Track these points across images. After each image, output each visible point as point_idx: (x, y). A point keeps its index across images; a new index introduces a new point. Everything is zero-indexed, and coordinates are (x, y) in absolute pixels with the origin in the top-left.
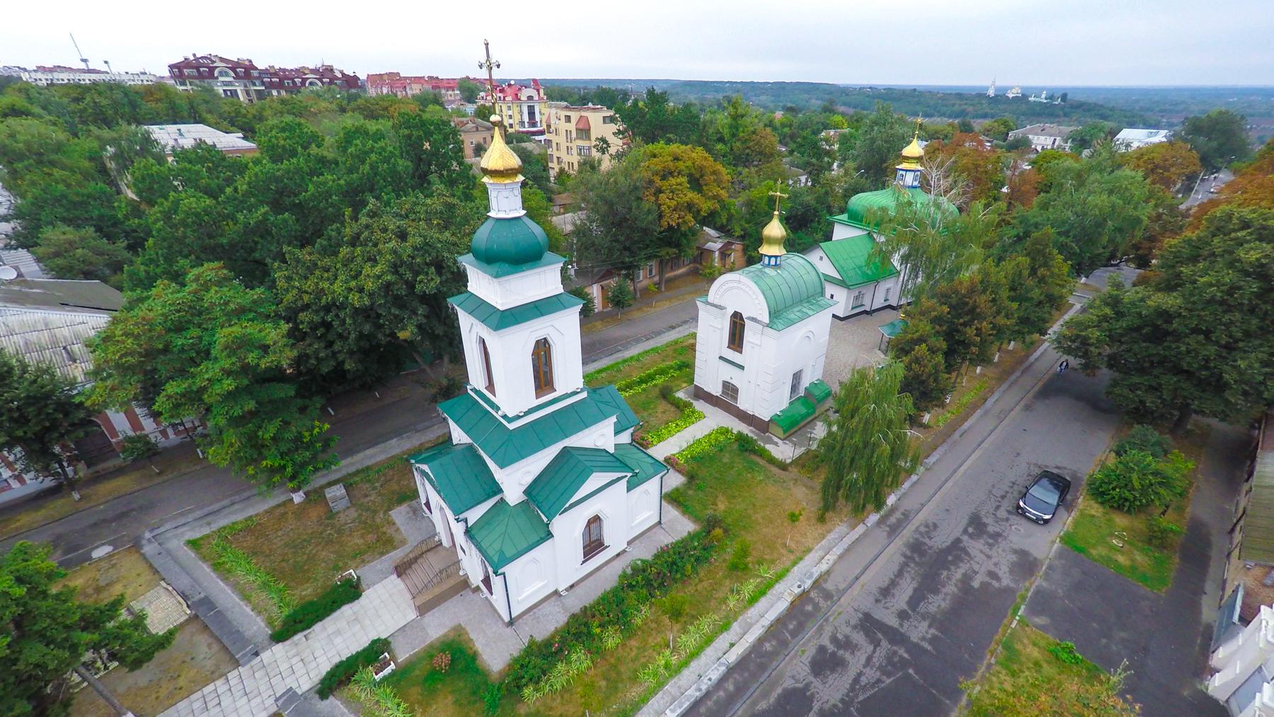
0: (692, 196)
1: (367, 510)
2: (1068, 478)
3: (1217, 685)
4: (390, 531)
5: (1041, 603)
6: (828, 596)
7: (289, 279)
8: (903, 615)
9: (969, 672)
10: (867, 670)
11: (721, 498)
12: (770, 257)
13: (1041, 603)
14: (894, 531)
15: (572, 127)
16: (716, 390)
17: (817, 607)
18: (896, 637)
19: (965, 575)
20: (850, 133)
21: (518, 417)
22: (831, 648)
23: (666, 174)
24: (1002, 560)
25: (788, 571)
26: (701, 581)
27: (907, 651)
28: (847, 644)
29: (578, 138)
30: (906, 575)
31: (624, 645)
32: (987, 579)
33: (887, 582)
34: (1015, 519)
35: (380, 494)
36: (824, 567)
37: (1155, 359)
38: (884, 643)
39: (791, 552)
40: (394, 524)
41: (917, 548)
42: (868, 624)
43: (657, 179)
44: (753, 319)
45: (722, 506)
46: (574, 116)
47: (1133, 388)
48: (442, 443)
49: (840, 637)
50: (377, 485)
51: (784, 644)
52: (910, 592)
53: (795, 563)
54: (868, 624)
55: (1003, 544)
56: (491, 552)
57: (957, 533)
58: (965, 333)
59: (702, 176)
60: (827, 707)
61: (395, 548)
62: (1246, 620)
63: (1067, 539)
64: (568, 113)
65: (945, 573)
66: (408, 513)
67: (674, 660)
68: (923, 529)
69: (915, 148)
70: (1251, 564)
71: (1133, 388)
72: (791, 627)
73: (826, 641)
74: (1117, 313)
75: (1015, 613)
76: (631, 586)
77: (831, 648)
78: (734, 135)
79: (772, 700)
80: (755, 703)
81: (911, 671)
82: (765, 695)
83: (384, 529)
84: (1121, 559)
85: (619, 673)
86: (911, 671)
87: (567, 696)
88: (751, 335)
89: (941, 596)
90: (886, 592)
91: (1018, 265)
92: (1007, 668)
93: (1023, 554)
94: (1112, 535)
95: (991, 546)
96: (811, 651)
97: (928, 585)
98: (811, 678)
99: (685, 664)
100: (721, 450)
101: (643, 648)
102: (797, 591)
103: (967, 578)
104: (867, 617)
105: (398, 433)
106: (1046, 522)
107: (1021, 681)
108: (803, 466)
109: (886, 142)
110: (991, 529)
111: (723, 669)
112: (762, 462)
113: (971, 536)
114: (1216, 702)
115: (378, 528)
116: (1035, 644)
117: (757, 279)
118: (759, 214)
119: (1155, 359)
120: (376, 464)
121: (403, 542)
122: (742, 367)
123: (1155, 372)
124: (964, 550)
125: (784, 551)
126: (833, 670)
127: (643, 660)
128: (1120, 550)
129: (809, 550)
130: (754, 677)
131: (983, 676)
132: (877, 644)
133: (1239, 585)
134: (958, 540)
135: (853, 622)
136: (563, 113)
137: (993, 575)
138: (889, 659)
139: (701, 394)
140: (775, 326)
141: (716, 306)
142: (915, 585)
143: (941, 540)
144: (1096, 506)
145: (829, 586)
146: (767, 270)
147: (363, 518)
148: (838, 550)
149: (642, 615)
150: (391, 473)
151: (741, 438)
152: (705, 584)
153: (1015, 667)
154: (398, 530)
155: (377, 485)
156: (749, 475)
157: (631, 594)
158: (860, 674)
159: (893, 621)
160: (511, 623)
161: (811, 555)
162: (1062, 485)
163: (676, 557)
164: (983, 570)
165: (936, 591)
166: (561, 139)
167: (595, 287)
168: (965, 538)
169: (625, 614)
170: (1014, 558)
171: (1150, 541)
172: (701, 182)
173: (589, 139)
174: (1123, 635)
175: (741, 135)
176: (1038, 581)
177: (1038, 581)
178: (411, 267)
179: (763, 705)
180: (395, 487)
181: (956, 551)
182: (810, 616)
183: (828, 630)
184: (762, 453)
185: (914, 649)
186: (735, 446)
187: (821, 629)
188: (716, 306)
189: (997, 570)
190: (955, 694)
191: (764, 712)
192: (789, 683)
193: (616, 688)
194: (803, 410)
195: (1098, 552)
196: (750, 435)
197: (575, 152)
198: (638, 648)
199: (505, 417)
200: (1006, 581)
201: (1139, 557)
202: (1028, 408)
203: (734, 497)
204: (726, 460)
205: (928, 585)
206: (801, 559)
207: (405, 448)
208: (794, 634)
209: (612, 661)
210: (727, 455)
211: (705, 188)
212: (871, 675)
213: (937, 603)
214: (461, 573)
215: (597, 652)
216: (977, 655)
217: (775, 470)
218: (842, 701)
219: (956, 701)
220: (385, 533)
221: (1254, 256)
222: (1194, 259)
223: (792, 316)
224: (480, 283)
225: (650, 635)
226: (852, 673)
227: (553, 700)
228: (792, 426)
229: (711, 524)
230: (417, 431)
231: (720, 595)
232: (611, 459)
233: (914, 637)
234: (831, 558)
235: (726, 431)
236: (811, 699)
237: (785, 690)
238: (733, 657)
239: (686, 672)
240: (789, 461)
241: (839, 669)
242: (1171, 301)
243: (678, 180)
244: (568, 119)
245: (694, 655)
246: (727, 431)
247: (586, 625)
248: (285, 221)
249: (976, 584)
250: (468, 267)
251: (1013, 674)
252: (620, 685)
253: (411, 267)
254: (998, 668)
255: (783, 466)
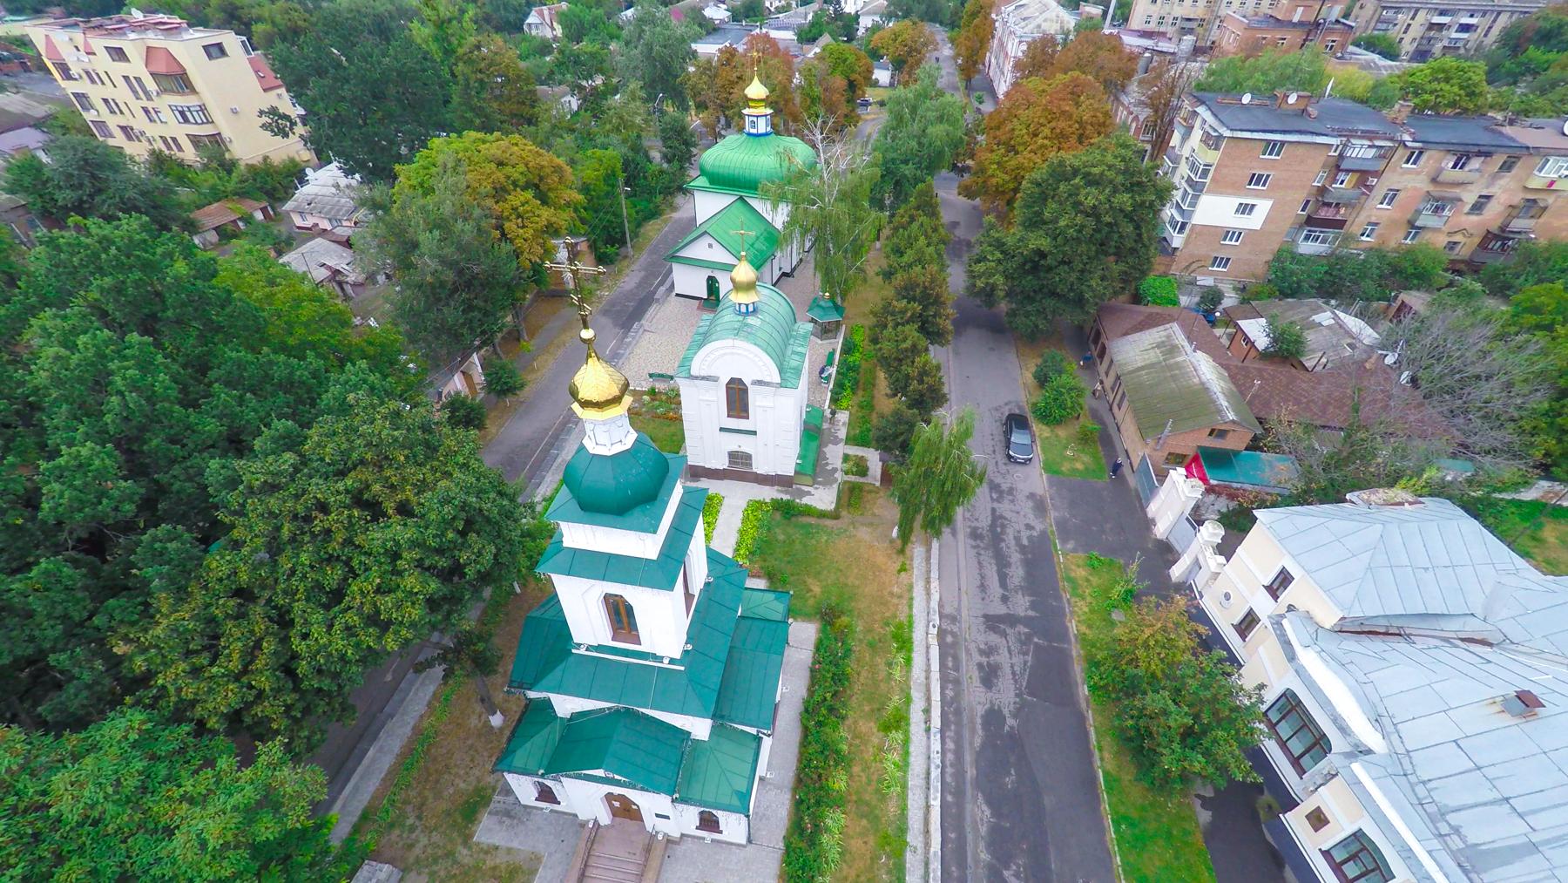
0: (546, 214)
1: (435, 861)
2: (1017, 412)
3: (1161, 530)
4: (501, 860)
5: (1064, 531)
6: (954, 619)
7: (196, 672)
8: (1005, 599)
9: (1059, 614)
10: (1015, 660)
11: (810, 581)
12: (747, 305)
13: (1064, 531)
14: (954, 533)
15: (137, 66)
16: (721, 463)
17: (953, 634)
18: (1012, 620)
19: (1015, 538)
20: (569, 9)
21: (685, 652)
22: (984, 660)
23: (500, 192)
24: (1027, 507)
25: (910, 616)
26: (858, 674)
27: (1025, 626)
28: (989, 651)
29: (165, 91)
30: (984, 563)
31: (851, 777)
32: (1028, 533)
33: (979, 578)
34: (1012, 468)
35: (429, 830)
36: (936, 597)
37: (1037, 288)
38: (1009, 631)
39: (900, 597)
40: (497, 848)
41: (975, 534)
42: (993, 623)
43: (489, 202)
44: (760, 383)
45: (817, 589)
46: (131, 43)
47: (1027, 314)
48: (520, 721)
49: (982, 646)
50: (410, 822)
51: (957, 682)
52: (996, 578)
53: (911, 607)
54: (993, 623)
55: (1021, 497)
56: (725, 800)
57: (989, 506)
58: (938, 324)
59: (541, 179)
60: (1012, 707)
61: (533, 872)
62: (1162, 482)
63: (1048, 468)
64: (114, 43)
65: (1003, 545)
66: (501, 823)
67: (895, 757)
68: (968, 515)
69: (756, 90)
70: (1149, 441)
71: (1027, 314)
72: (950, 664)
73: (977, 658)
74: (1002, 252)
75: (1056, 550)
76: (820, 724)
77: (984, 660)
78: (448, 52)
79: (980, 732)
80: (971, 744)
81: (1036, 640)
82: (973, 731)
83: (490, 863)
84: (1079, 466)
85: (867, 804)
86: (1036, 640)
87: (847, 857)
88: (756, 398)
89: (1013, 567)
90: (983, 587)
91: (922, 225)
92: (1078, 596)
93: (1032, 496)
94: (1066, 448)
95: (1012, 501)
96: (976, 674)
97: (1002, 562)
98: (990, 694)
99: (907, 753)
100: (769, 530)
101: (866, 768)
102: (935, 631)
103: (1018, 539)
104: (986, 616)
105: (367, 734)
106: (1030, 460)
107: (1089, 599)
108: (849, 505)
109: (665, 47)
110: (1005, 487)
111: (939, 736)
112: (812, 521)
113: (998, 500)
114: (1160, 542)
115: (477, 869)
116: (1079, 566)
117: (740, 331)
118: (598, 198)
119: (1037, 288)
120: (377, 797)
121: (536, 859)
122: (754, 433)
123: (1038, 298)
124: (1001, 517)
125: (895, 601)
126: (997, 677)
127: (875, 777)
128: (1074, 459)
129: (910, 588)
130: (959, 724)
131: (1071, 612)
132: (1004, 635)
133: (1144, 457)
134: (993, 510)
135: (982, 628)
136: (99, 43)
137: (1029, 527)
138: (1023, 643)
139: (697, 473)
140: (789, 384)
141: (703, 378)
142: (995, 568)
143: (984, 522)
144: (1044, 427)
145: (948, 610)
146: (751, 320)
147: (442, 873)
148: (934, 575)
149: (842, 737)
150: (412, 793)
151: (778, 506)
152: (864, 674)
153: (1080, 591)
154: (509, 850)
155: (410, 822)
156: (814, 542)
157: (828, 730)
158: (1012, 666)
159: (999, 609)
160: (749, 841)
161: (915, 590)
162: (1016, 421)
163: (833, 669)
164: (1022, 528)
165: (1008, 565)
166: (122, 94)
167: (456, 377)
168: (996, 505)
169: (838, 752)
170: (1030, 504)
171: (1086, 442)
172: (542, 187)
173: (193, 91)
174: (1109, 526)
175: (461, 51)
176: (1053, 514)
177: (1053, 514)
178: (440, 551)
179: (978, 742)
180: (443, 806)
181: (997, 519)
182: (955, 644)
183: (972, 646)
184: (808, 511)
185: (1027, 621)
186: (778, 516)
187: (967, 650)
188: (703, 378)
189: (1027, 521)
190: (1063, 635)
191: (983, 745)
192: (980, 711)
193: (876, 817)
194: (814, 444)
195: (1065, 467)
196: (786, 497)
197: (167, 115)
198: (863, 771)
199: (672, 661)
200: (1039, 527)
201: (1086, 459)
202: (956, 353)
203: (819, 573)
204: (781, 537)
205: (1002, 562)
206: (912, 599)
207: (397, 750)
208: (957, 668)
209: (854, 798)
210: (777, 530)
211: (551, 195)
212: (1018, 660)
213: (1017, 573)
214: (660, 837)
215: (839, 802)
216: (1059, 598)
217: (829, 523)
218: (1017, 695)
219: (1069, 642)
220: (494, 868)
221: (1091, 202)
222: (1044, 198)
223: (793, 364)
224: (578, 535)
225: (862, 752)
226: (1008, 670)
227: (841, 870)
228: (813, 467)
229: (828, 616)
230: (392, 716)
231: (882, 675)
232: (749, 622)
233: (1022, 614)
234: (935, 585)
235: (755, 506)
236: (1000, 711)
237: (982, 716)
238: (936, 722)
239: (912, 759)
240: (833, 506)
241: (999, 673)
242: (1039, 241)
243: (522, 199)
244: (118, 54)
245: (906, 742)
246: (761, 503)
247: (822, 788)
248: (47, 573)
249: (1025, 542)
250: (564, 526)
251: (1084, 599)
252: (877, 812)
253: (440, 551)
254: (1073, 600)
255: (834, 515)
